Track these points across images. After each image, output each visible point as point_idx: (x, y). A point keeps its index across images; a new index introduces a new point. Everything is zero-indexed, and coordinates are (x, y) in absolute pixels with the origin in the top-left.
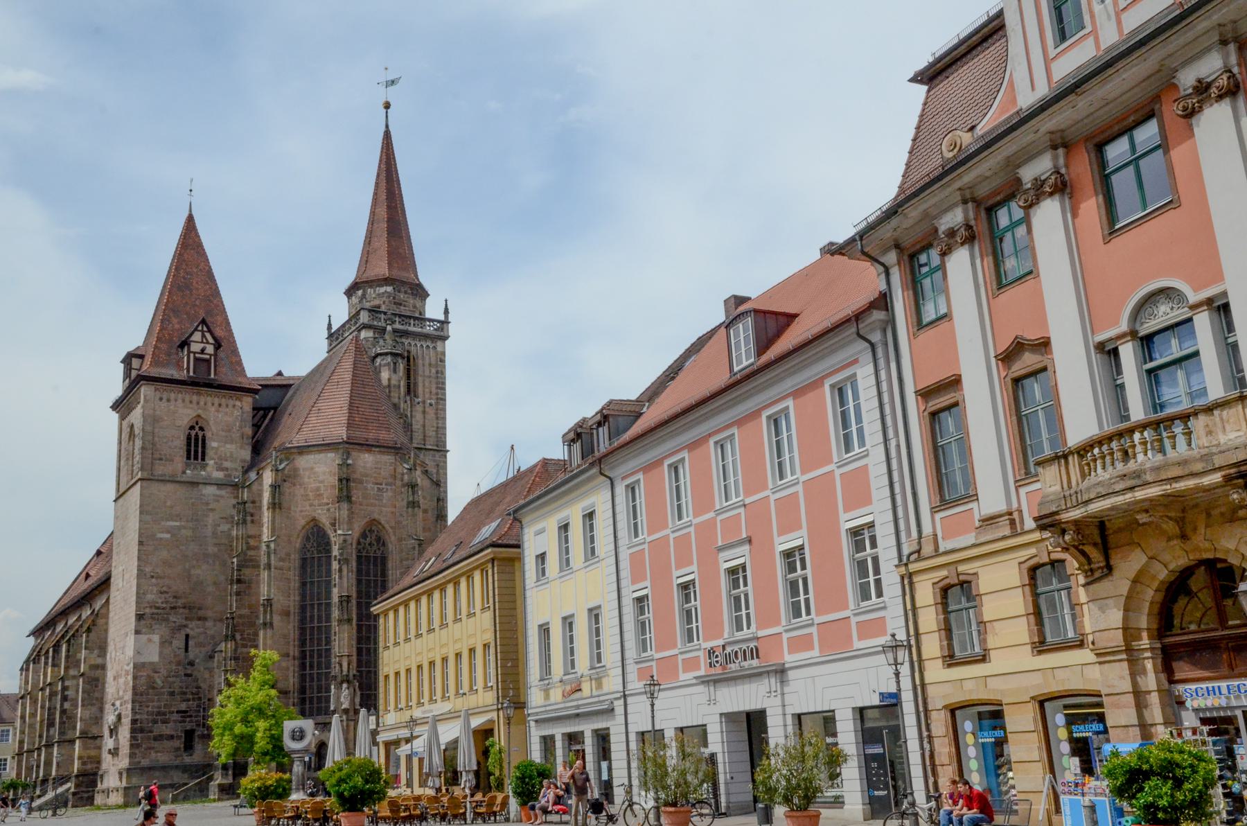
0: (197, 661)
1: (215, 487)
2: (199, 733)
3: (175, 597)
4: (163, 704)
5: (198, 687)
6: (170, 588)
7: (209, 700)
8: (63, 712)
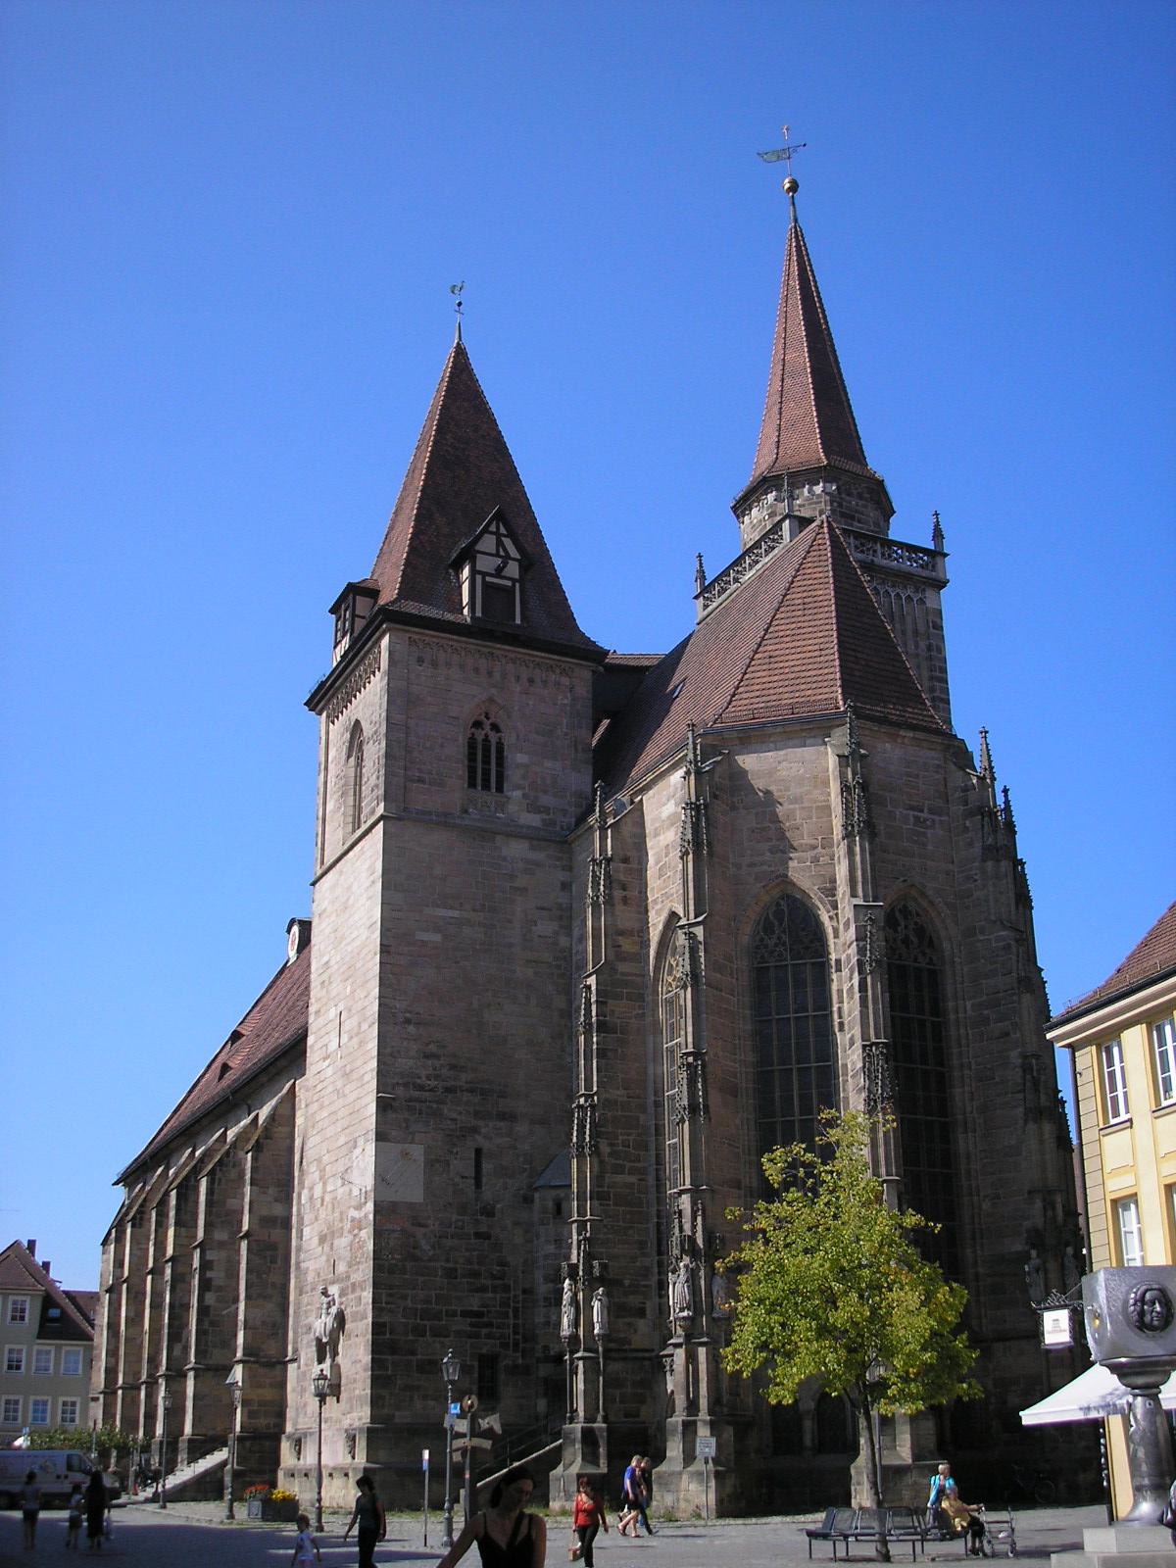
0: (498, 1206)
1: (525, 844)
2: (508, 1362)
3: (453, 1067)
4: (433, 1293)
5: (503, 1264)
6: (444, 1047)
7: (525, 1291)
8: (203, 1311)
